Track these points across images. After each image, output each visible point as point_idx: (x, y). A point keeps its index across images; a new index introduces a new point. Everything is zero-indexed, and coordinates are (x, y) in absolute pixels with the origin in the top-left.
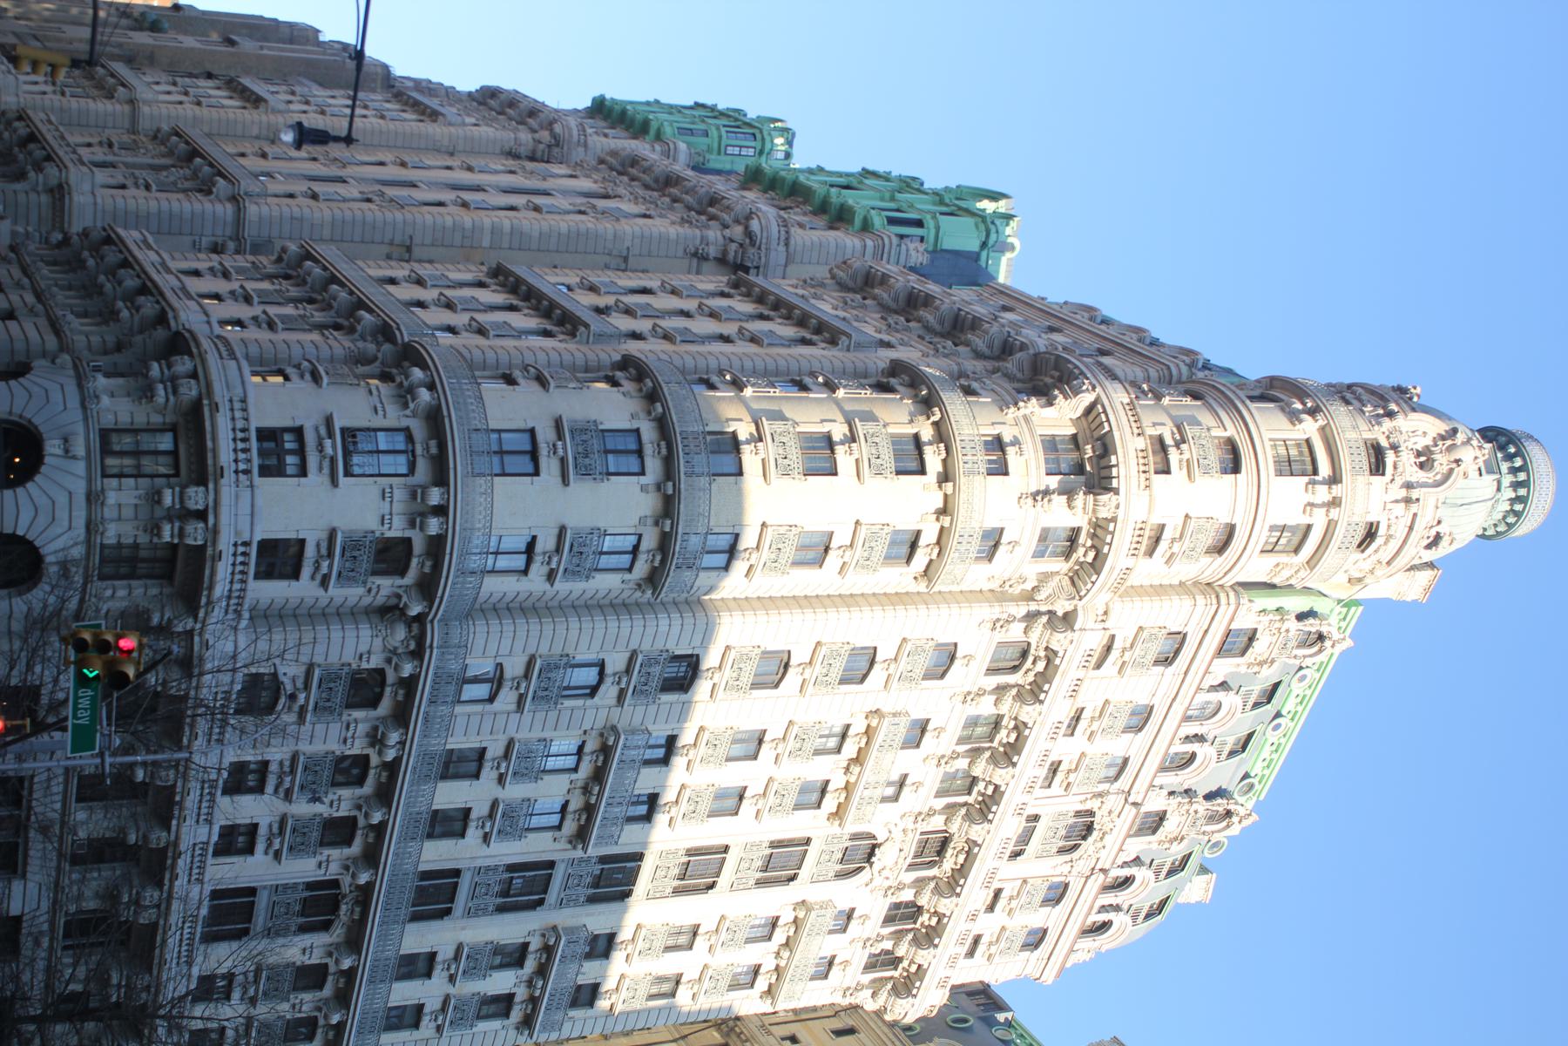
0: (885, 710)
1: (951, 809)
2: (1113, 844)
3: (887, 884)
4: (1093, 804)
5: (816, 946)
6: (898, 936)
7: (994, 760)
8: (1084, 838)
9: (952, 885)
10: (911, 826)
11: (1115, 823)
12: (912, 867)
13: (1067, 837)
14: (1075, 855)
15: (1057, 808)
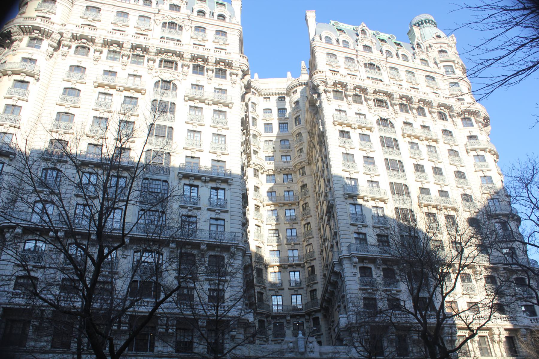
0: (333, 121)
1: (366, 100)
2: (375, 56)
3: (394, 114)
4: (362, 64)
5: (418, 131)
6: (411, 109)
7: (346, 90)
8: (374, 65)
9: (390, 95)
10: (373, 110)
11: (368, 57)
12: (387, 108)
13: (375, 69)
14: (380, 66)
15: (363, 72)
